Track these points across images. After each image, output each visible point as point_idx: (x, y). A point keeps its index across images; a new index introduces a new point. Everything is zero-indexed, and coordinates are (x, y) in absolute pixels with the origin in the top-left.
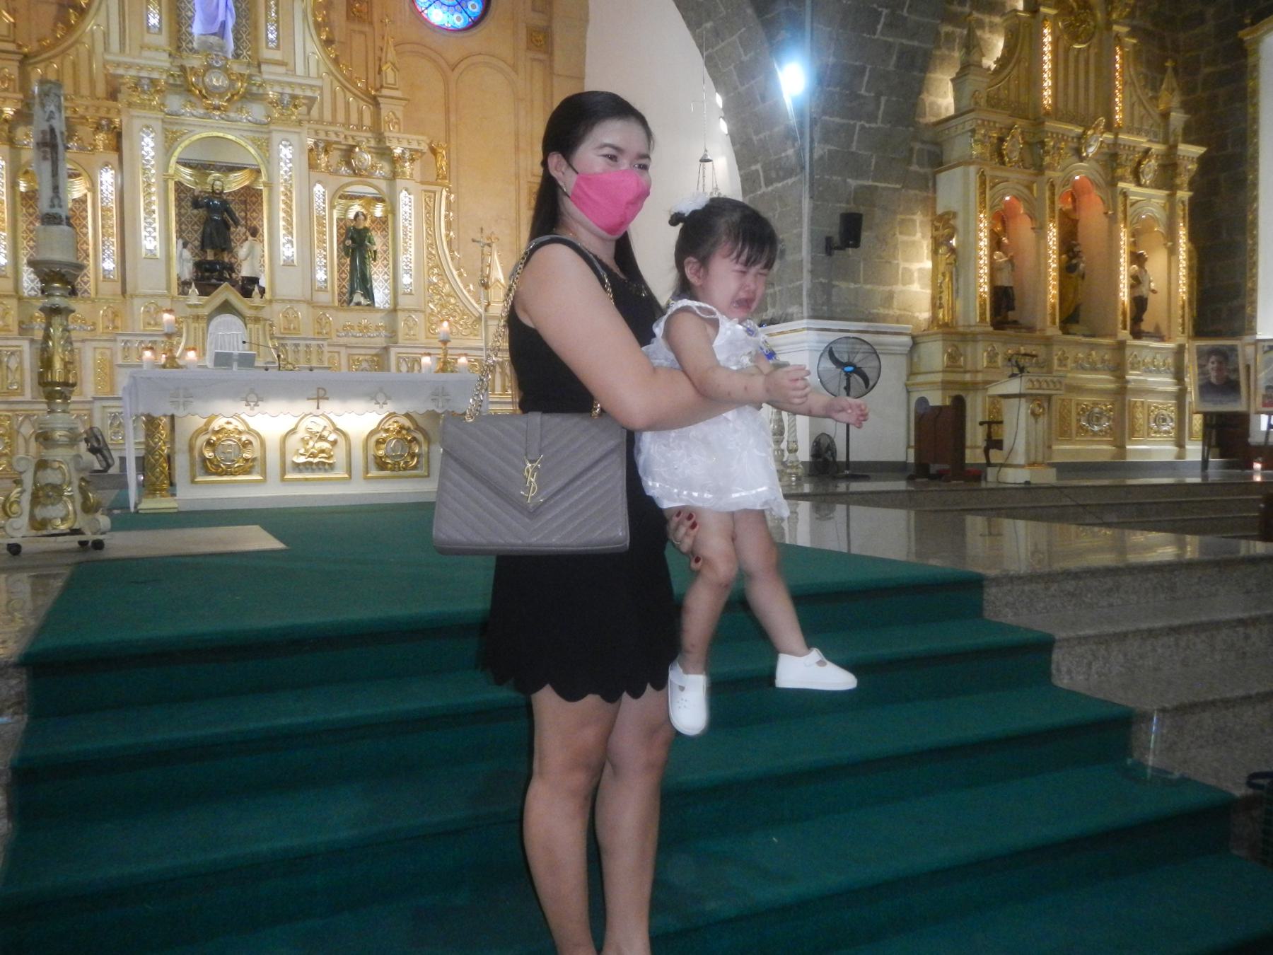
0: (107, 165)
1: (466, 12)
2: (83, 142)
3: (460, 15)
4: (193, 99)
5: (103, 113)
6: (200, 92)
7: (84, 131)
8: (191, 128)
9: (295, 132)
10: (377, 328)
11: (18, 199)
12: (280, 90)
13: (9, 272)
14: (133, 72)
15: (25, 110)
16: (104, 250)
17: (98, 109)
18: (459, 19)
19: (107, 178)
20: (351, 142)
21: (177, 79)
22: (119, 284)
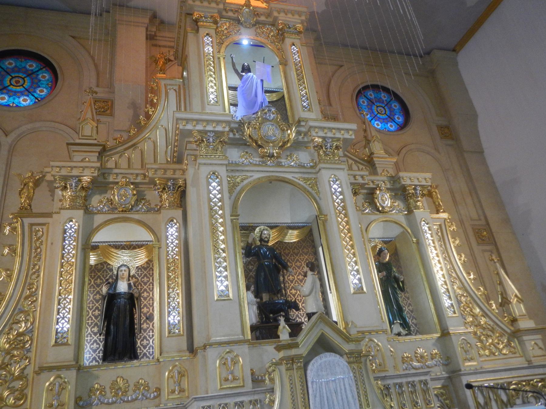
0: (172, 221)
1: (394, 122)
2: (150, 204)
3: (391, 124)
4: (249, 150)
5: (169, 174)
6: (256, 143)
7: (152, 195)
8: (249, 174)
9: (341, 169)
10: (433, 357)
11: (87, 274)
12: (324, 135)
13: (71, 339)
14: (200, 127)
15: (101, 179)
16: (169, 303)
17: (165, 170)
18: (391, 126)
19: (172, 231)
20: (372, 185)
21: (237, 134)
22: (185, 338)
